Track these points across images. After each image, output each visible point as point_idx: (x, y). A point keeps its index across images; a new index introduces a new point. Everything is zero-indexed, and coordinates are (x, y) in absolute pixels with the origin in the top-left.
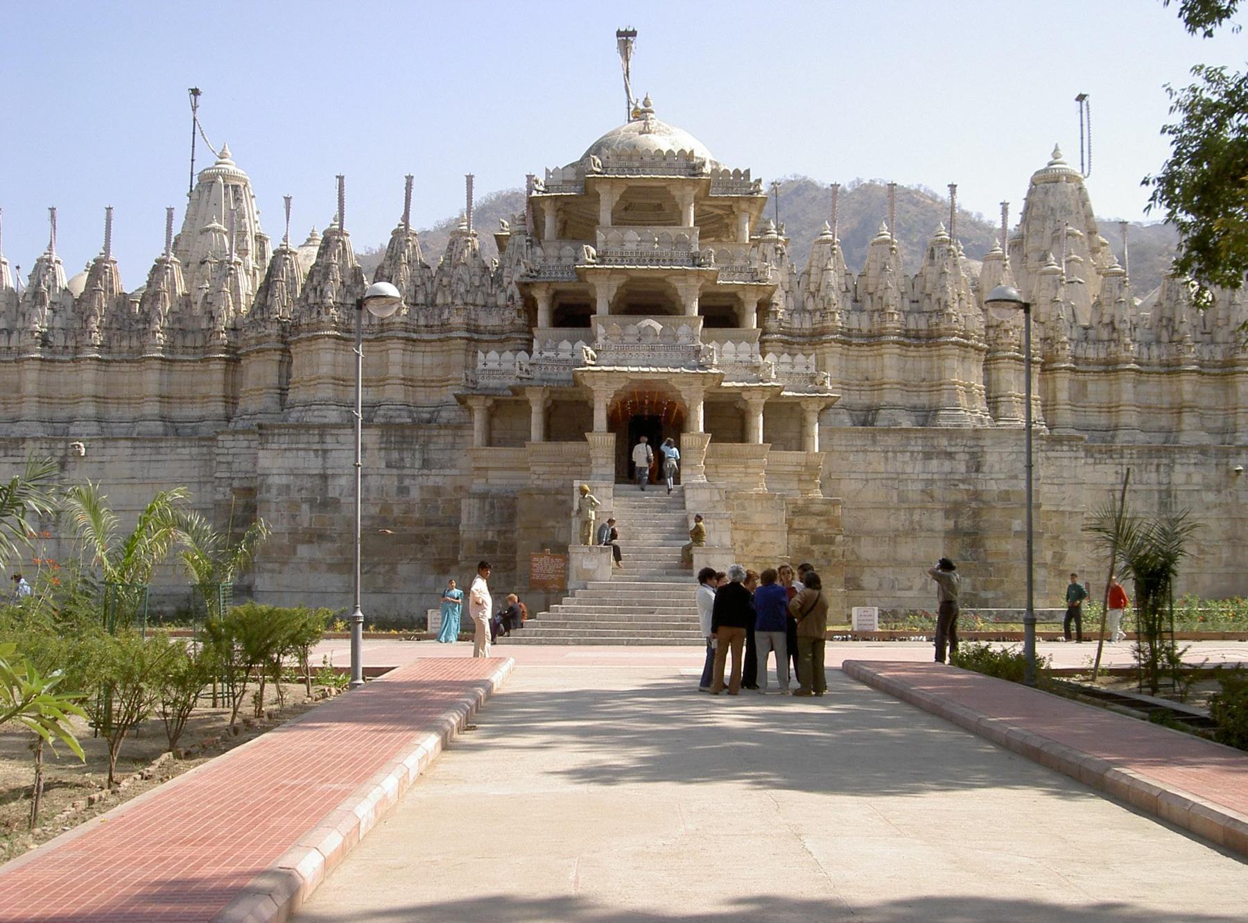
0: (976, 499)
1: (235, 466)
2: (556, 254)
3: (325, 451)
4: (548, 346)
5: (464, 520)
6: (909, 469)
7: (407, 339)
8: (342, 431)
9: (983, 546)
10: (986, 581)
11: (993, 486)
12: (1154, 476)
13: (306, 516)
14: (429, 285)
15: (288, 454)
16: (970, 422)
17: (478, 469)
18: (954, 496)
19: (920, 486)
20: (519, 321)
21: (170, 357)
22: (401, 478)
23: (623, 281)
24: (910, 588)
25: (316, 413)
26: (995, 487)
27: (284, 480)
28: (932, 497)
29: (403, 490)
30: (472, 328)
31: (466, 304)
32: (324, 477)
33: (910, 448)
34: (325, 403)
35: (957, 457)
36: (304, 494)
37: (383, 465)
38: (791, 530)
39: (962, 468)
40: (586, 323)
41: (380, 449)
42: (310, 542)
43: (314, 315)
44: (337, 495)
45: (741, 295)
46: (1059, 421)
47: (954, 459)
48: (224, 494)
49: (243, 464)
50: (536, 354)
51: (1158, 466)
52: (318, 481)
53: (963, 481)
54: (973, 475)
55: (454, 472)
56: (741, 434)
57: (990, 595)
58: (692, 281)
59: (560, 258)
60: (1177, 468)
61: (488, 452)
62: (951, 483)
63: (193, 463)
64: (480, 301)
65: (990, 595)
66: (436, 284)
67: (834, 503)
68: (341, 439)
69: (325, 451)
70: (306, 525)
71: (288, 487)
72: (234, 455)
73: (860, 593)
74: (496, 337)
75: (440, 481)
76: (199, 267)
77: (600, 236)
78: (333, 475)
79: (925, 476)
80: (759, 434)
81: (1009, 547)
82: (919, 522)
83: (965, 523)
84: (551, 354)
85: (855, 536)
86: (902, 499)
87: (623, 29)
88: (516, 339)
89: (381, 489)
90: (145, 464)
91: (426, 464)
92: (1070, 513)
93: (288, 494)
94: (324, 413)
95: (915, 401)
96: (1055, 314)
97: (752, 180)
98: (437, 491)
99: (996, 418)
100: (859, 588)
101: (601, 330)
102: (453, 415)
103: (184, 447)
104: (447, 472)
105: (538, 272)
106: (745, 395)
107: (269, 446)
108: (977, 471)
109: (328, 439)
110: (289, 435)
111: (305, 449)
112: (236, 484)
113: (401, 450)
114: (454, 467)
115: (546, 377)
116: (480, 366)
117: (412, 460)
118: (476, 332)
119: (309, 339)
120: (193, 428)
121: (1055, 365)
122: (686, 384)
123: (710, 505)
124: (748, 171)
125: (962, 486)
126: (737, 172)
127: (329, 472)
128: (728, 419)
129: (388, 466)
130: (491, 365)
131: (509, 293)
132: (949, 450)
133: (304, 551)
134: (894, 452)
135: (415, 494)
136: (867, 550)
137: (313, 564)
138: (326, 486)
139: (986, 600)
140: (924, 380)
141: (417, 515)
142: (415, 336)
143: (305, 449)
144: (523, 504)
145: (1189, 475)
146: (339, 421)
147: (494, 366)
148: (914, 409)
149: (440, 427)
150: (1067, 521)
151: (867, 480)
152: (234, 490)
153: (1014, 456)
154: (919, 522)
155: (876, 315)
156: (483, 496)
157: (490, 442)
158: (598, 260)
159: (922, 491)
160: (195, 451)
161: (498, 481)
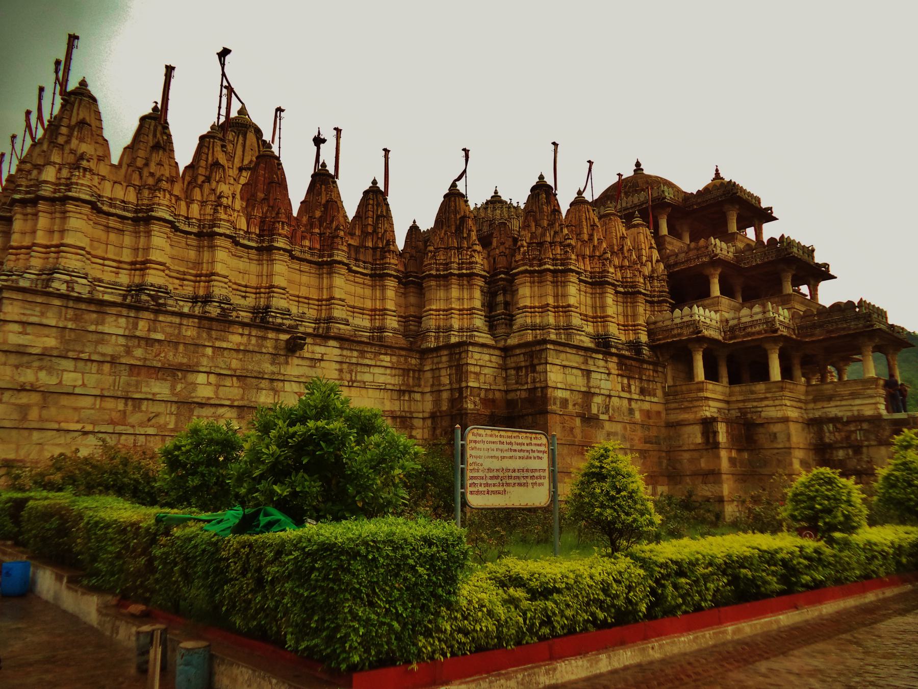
1: (482, 378)
3: (589, 372)
22: (630, 400)
25: (578, 337)
36: (578, 409)
37: (620, 389)
41: (618, 375)
48: (475, 403)
55: (655, 400)
61: (710, 386)
63: (394, 372)
69: (589, 372)
72: (481, 366)
90: (353, 367)
91: (643, 392)
103: (386, 354)
109: (591, 362)
113: (629, 378)
127: (593, 390)
135: (637, 415)
160: (394, 359)
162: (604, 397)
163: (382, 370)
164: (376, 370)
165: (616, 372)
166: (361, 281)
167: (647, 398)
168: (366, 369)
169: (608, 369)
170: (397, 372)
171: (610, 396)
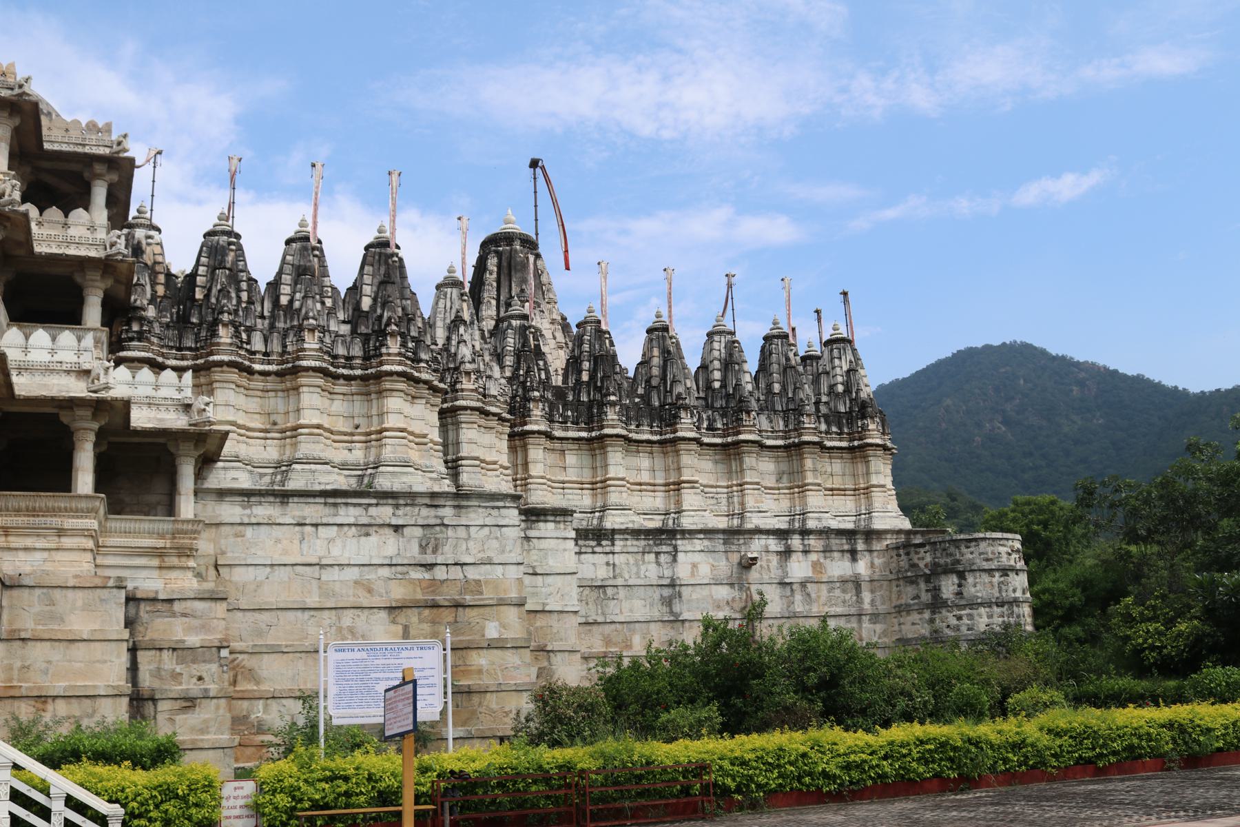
12: (653, 567)
16: (420, 483)
26: (461, 576)
33: (339, 520)
45: (78, 279)
51: (658, 554)
56: (61, 480)
60: (681, 556)
80: (84, 480)
82: (352, 631)
97: (114, 137)
106: (65, 418)
121: (527, 428)
124: (108, 129)
126: (92, 127)
132: (394, 522)
145: (694, 566)
148: (343, 466)
151: (272, 565)
159: (356, 582)
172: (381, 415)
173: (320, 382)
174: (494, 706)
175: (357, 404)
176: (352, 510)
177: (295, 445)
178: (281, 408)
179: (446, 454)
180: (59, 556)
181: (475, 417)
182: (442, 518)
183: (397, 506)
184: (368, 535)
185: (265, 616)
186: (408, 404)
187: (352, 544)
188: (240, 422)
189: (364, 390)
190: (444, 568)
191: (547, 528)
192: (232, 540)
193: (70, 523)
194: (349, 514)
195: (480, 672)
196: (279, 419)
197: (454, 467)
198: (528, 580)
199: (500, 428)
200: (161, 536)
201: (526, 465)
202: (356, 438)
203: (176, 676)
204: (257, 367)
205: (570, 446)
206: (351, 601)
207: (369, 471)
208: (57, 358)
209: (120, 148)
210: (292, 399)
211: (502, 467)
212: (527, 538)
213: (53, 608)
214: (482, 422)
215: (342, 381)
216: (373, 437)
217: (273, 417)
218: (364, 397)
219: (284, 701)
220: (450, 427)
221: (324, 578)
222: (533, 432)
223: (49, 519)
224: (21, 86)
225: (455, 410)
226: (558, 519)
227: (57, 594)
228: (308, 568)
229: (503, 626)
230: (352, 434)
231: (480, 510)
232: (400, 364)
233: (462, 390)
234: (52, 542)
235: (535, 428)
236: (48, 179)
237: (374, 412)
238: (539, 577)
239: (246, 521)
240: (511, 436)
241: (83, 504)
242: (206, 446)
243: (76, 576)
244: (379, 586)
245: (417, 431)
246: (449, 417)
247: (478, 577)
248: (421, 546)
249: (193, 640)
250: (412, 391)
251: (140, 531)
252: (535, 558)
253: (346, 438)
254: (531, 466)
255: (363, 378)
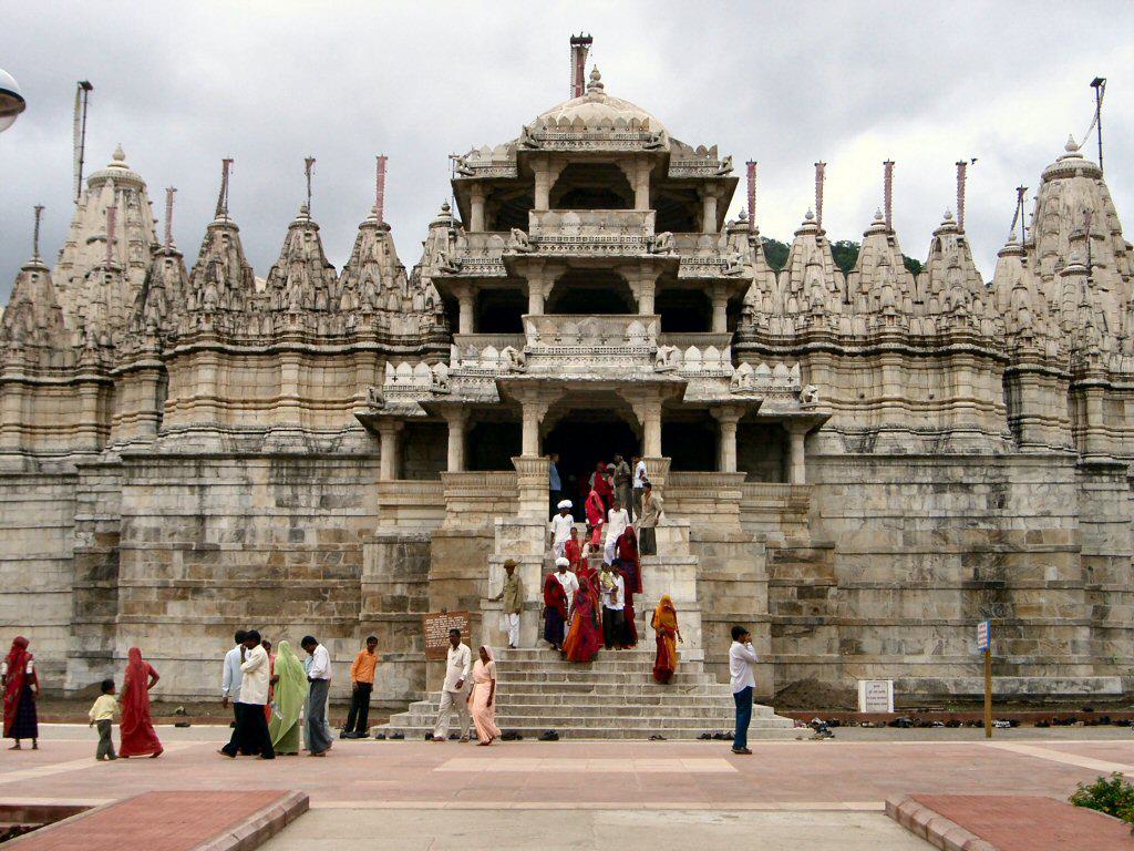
0: (1000, 541)
1: (100, 507)
2: (482, 245)
4: (469, 353)
5: (367, 572)
6: (916, 506)
7: (305, 352)
8: (224, 463)
9: (1011, 599)
10: (1015, 643)
11: (1021, 525)
13: (179, 567)
14: (332, 287)
15: (158, 490)
16: (986, 446)
17: (384, 507)
18: (971, 538)
19: (929, 526)
20: (439, 329)
21: (31, 378)
23: (562, 273)
24: (921, 652)
25: (193, 442)
26: (1023, 527)
27: (153, 523)
28: (946, 539)
29: (296, 534)
30: (383, 337)
31: (375, 309)
32: (201, 518)
33: (918, 480)
34: (204, 429)
35: (976, 489)
36: (177, 540)
38: (772, 584)
39: (982, 504)
40: (518, 328)
42: (184, 598)
43: (194, 323)
44: (216, 541)
45: (708, 292)
46: (1092, 447)
47: (972, 492)
49: (106, 506)
50: (454, 365)
52: (193, 524)
53: (984, 519)
54: (997, 512)
56: (710, 462)
57: (1020, 659)
58: (646, 270)
59: (486, 250)
62: (967, 520)
63: (55, 504)
64: (392, 305)
65: (1020, 659)
66: (340, 286)
67: (829, 547)
68: (223, 472)
69: (202, 487)
70: (178, 578)
71: (157, 531)
72: (98, 493)
73: (858, 659)
74: (412, 349)
75: (341, 523)
76: (84, 282)
77: (533, 220)
78: (211, 515)
79: (937, 514)
81: (1043, 600)
82: (931, 572)
83: (988, 571)
84: (473, 363)
85: (852, 590)
86: (908, 541)
87: (577, 36)
88: (435, 350)
89: (270, 533)
91: (325, 502)
92: (1115, 557)
93: (157, 539)
94: (202, 441)
95: (920, 421)
96: (1084, 321)
97: (720, 158)
98: (339, 535)
99: (1020, 444)
100: (859, 651)
101: (530, 328)
102: (357, 443)
103: (46, 485)
104: (349, 511)
105: (460, 266)
106: (714, 413)
107: (135, 481)
108: (1001, 505)
109: (207, 472)
110: (159, 467)
111: (178, 485)
112: (100, 528)
113: (294, 485)
114: (358, 505)
115: (467, 392)
116: (389, 382)
117: (308, 499)
118: (388, 342)
119: (186, 353)
120: (59, 463)
121: (1086, 381)
122: (638, 395)
123: (671, 547)
125: (982, 526)
126: (702, 150)
127: (207, 512)
128: (693, 439)
129: (280, 504)
130: (401, 381)
131: (427, 295)
132: (965, 481)
133: (176, 609)
134: (898, 484)
135: (311, 540)
136: (868, 607)
137: (187, 624)
138: (204, 530)
139: (1016, 667)
140: (931, 397)
141: (313, 564)
142: (313, 347)
143: (178, 485)
144: (438, 550)
146: (219, 451)
147: (407, 381)
148: (921, 431)
149: (342, 458)
150: (1110, 569)
151: (865, 518)
152: (98, 536)
153: (1046, 488)
154: (931, 572)
155: (873, 318)
156: (389, 542)
157: (402, 473)
158: (530, 247)
159: (934, 532)
160: (58, 490)
161: (409, 525)
162: (234, 520)
163: (38, 506)
164: (31, 506)
165: (265, 481)
166: (59, 393)
167: (334, 512)
168: (15, 506)
169: (244, 478)
170: (60, 504)
171: (248, 517)
172: (952, 386)
173: (900, 361)
174: (1052, 638)
175: (931, 377)
176: (929, 471)
177: (880, 415)
178: (867, 384)
179: (1009, 412)
180: (716, 518)
181: (1036, 378)
182: (1007, 477)
183: (968, 466)
184: (945, 492)
185: (857, 561)
186: (976, 376)
187: (929, 501)
188: (835, 397)
189: (937, 364)
190: (1009, 520)
191: (1104, 482)
192: (831, 496)
193: (722, 494)
194: (926, 476)
195: (1040, 609)
196: (866, 392)
197: (1016, 425)
198: (1084, 528)
199: (1060, 386)
200: (781, 498)
201: (1086, 415)
202: (930, 407)
203: (794, 608)
204: (847, 349)
205: (1129, 396)
206: (931, 548)
207: (944, 436)
208: (705, 367)
209: (727, 168)
210: (876, 375)
211: (1062, 421)
212: (1084, 491)
213: (714, 557)
214: (1043, 382)
215: (917, 358)
216: (946, 406)
217: (861, 391)
218: (937, 371)
219: (877, 629)
220: (1013, 387)
221: (907, 529)
222: (1092, 385)
223: (708, 492)
224: (656, 140)
225: (1016, 373)
226: (1113, 472)
227: (717, 547)
228: (893, 521)
229: (1062, 571)
230: (928, 404)
231: (1040, 470)
232: (968, 341)
233: (1024, 354)
234: (710, 508)
235: (1094, 381)
236: (667, 195)
237: (946, 384)
238: (1096, 526)
239: (843, 481)
240: (1072, 389)
241: (732, 480)
242: (813, 426)
243: (730, 534)
244: (953, 534)
245: (984, 400)
246: (1011, 379)
247: (1039, 528)
248: (988, 501)
249: (809, 580)
250: (979, 364)
251: (770, 494)
252: (1091, 508)
253: (922, 407)
254: (1091, 417)
255: (937, 355)
